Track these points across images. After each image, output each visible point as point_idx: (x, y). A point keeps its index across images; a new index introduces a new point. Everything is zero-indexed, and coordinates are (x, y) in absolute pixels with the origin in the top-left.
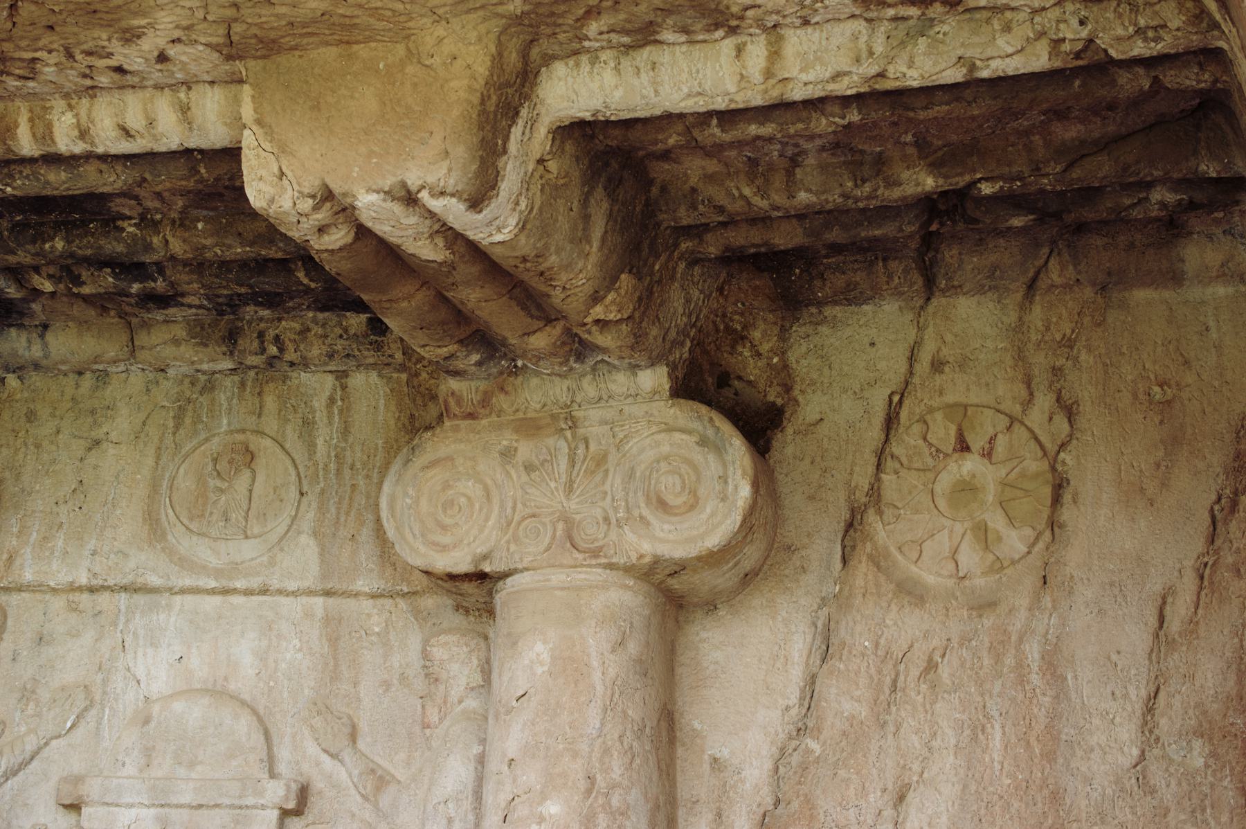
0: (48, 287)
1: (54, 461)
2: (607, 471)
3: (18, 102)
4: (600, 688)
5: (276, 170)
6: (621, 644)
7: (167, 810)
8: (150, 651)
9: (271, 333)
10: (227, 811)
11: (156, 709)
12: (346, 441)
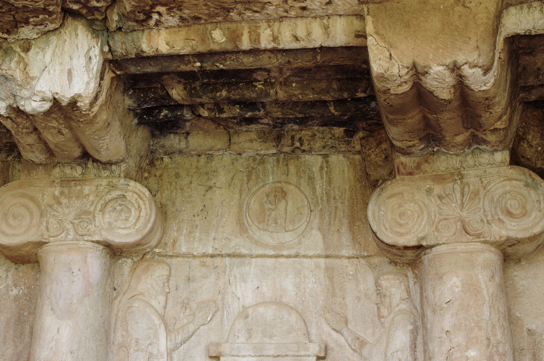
0: (206, 114)
1: (190, 196)
2: (480, 198)
3: (243, 24)
4: (487, 298)
5: (388, 55)
6: (493, 277)
7: (261, 358)
8: (243, 284)
9: (298, 136)
10: (291, 358)
11: (250, 311)
12: (330, 186)
